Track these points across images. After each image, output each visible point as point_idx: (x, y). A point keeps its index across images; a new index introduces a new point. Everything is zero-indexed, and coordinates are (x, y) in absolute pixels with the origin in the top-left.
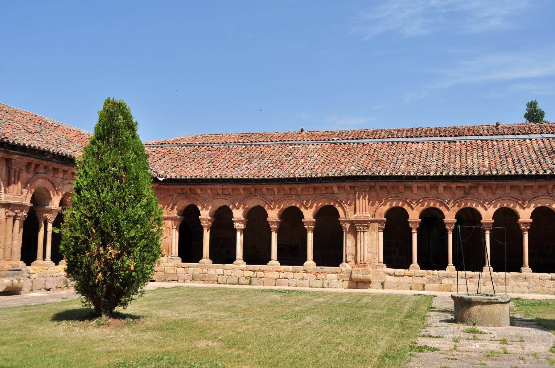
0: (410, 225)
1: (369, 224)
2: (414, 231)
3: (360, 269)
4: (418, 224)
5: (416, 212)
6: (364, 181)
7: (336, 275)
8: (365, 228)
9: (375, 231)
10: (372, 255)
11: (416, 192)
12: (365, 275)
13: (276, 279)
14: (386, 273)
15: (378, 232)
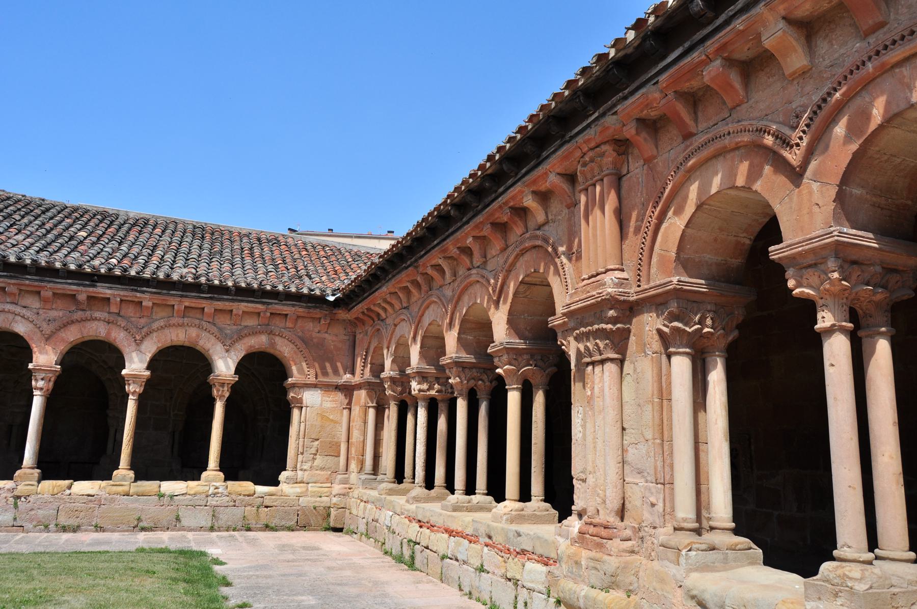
0: (791, 283)
1: (614, 321)
2: (825, 319)
3: (585, 554)
4: (831, 264)
5: (815, 186)
6: (585, 124)
7: (544, 569)
8: (601, 345)
9: (646, 355)
10: (642, 483)
11: (796, 60)
12: (594, 593)
13: (443, 557)
14: (693, 597)
15: (669, 357)
